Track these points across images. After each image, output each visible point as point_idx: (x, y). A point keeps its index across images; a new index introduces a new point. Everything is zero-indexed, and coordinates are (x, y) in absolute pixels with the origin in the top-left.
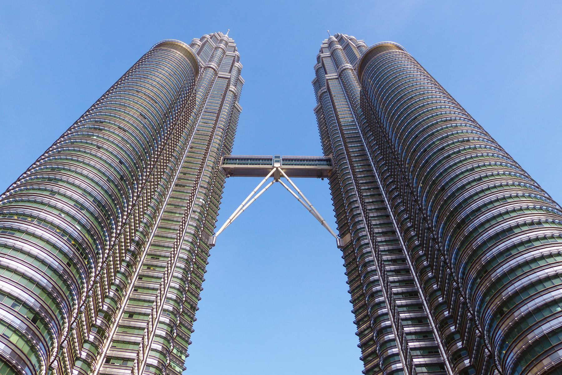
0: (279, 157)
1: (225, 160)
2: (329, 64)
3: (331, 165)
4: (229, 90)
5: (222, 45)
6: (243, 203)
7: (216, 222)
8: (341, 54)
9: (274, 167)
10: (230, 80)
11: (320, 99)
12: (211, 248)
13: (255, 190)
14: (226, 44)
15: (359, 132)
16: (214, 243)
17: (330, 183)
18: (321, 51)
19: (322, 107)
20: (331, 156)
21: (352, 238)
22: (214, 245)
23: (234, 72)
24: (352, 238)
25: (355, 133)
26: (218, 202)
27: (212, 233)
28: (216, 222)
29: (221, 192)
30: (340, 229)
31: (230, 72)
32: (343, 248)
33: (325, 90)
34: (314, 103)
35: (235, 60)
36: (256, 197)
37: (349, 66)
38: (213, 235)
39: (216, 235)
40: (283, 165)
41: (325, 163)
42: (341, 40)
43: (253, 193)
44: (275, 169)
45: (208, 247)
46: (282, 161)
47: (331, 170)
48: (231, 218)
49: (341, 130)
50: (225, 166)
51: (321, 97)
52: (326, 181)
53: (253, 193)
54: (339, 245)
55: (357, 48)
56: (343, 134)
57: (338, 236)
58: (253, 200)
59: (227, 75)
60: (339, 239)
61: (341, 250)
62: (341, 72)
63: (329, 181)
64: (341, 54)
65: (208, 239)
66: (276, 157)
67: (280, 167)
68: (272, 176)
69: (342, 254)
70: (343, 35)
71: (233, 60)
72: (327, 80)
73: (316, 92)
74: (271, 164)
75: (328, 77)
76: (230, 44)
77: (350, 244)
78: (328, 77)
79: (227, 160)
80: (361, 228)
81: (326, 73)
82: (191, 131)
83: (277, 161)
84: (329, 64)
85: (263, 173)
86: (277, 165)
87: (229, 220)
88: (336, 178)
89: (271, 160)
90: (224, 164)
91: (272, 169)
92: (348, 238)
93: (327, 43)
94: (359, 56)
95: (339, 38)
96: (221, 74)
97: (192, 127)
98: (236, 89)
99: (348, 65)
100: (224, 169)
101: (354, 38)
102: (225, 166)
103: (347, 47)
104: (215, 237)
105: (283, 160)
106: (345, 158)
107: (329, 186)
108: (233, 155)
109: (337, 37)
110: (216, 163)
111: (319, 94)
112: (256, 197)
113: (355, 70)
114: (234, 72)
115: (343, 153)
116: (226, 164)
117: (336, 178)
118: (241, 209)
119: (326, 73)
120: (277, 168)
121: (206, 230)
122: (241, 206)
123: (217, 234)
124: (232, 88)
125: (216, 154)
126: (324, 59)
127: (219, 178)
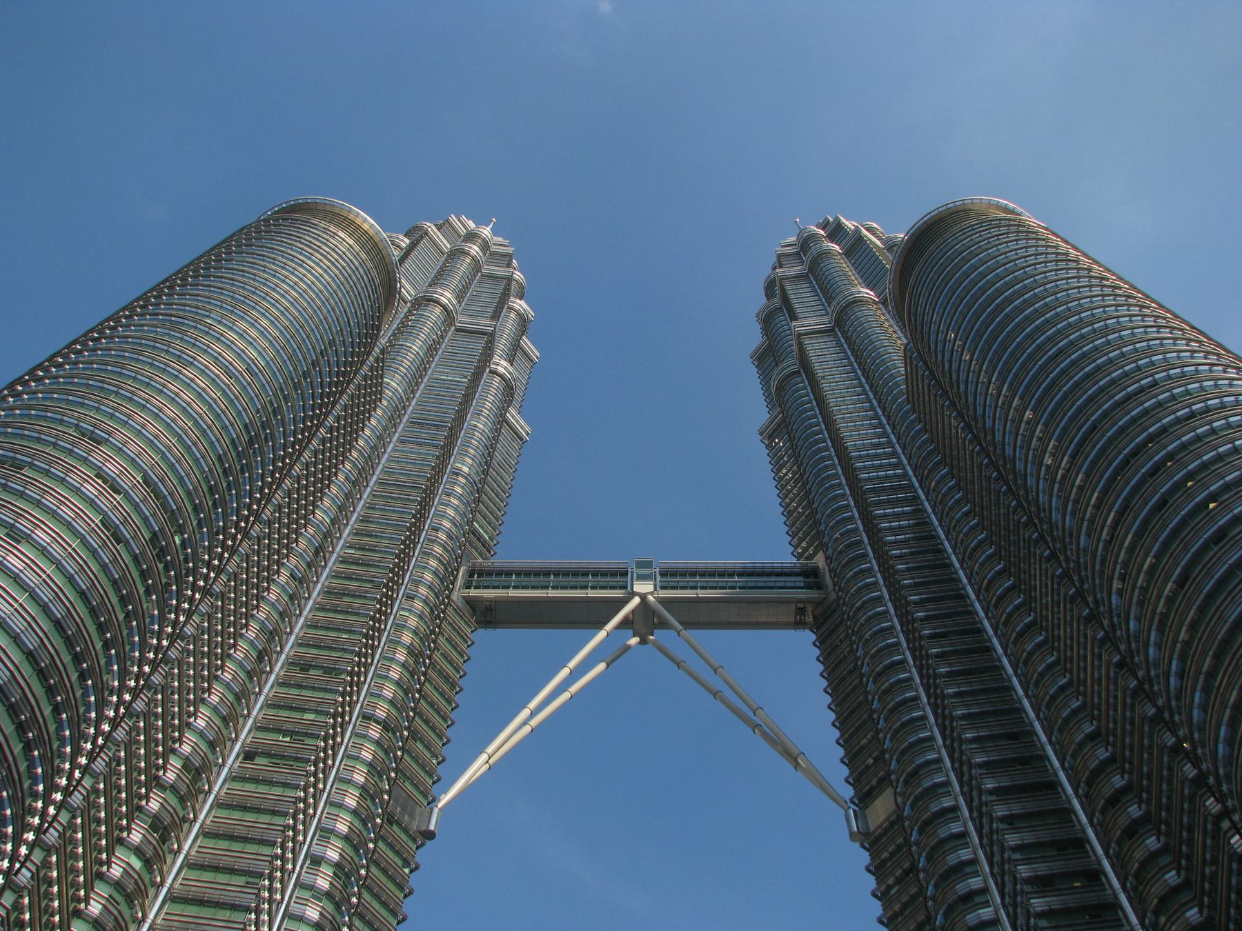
0: (649, 565)
1: (471, 575)
2: (800, 296)
3: (819, 586)
4: (490, 372)
5: (474, 249)
6: (533, 704)
7: (439, 763)
8: (843, 268)
9: (633, 594)
10: (494, 339)
11: (778, 395)
12: (423, 845)
13: (573, 663)
14: (485, 246)
15: (905, 474)
16: (432, 827)
17: (821, 642)
18: (780, 262)
19: (783, 420)
20: (820, 560)
21: (899, 799)
22: (430, 835)
23: (509, 324)
24: (899, 799)
25: (895, 476)
26: (449, 701)
27: (425, 796)
28: (439, 763)
29: (458, 672)
30: (855, 780)
31: (496, 316)
32: (869, 840)
33: (794, 368)
34: (759, 413)
35: (509, 290)
36: (574, 688)
37: (867, 293)
38: (429, 804)
39: (440, 805)
40: (662, 588)
41: (800, 581)
42: (836, 232)
43: (565, 672)
44: (637, 600)
45: (414, 840)
46: (659, 578)
47: (818, 603)
48: (490, 749)
49: (853, 482)
50: (473, 593)
51: (780, 389)
52: (806, 638)
53: (565, 672)
54: (855, 829)
55: (888, 250)
56: (853, 482)
57: (852, 802)
58: (566, 696)
59: (487, 324)
60: (854, 811)
61: (863, 846)
62: (842, 311)
63: (813, 637)
64: (843, 268)
65: (412, 816)
66: (640, 565)
67: (652, 593)
68: (625, 623)
69: (865, 857)
70: (843, 220)
71: (505, 289)
72: (799, 335)
73: (765, 380)
74: (625, 587)
75: (799, 326)
76: (494, 249)
77: (892, 824)
78: (799, 326)
79: (479, 575)
80: (929, 763)
81: (793, 317)
82: (363, 474)
83: (642, 578)
84: (800, 296)
85: (595, 615)
86: (643, 587)
87: (484, 757)
88: (841, 623)
89: (625, 574)
90: (468, 587)
91: (625, 601)
92: (882, 808)
93: (795, 245)
94: (888, 261)
95: (830, 228)
96: (462, 320)
97: (370, 461)
98: (511, 369)
99: (862, 290)
100: (470, 602)
101: (876, 226)
102: (473, 593)
103: (855, 247)
104: (436, 810)
105: (663, 574)
106: (865, 555)
107: (817, 652)
108: (498, 560)
109: (824, 226)
110: (447, 578)
111: (774, 383)
112: (574, 688)
113: (884, 303)
114: (509, 324)
115: (860, 542)
116: (477, 587)
117: (841, 623)
118: (525, 723)
119: (793, 317)
120: (643, 597)
121: (407, 784)
122: (525, 713)
123: (445, 799)
124: (501, 365)
125: (444, 547)
126: (785, 283)
127: (453, 627)
